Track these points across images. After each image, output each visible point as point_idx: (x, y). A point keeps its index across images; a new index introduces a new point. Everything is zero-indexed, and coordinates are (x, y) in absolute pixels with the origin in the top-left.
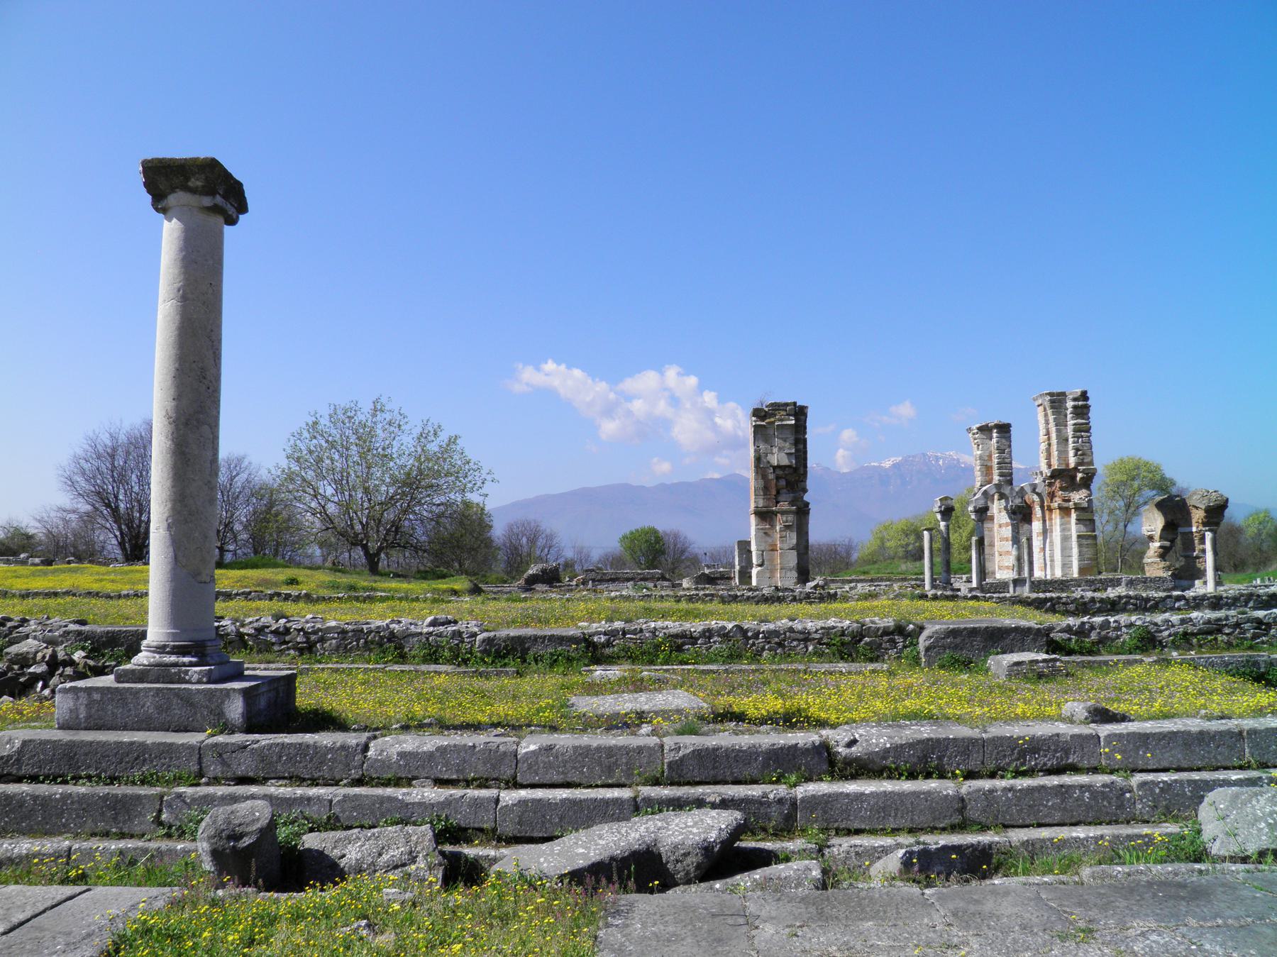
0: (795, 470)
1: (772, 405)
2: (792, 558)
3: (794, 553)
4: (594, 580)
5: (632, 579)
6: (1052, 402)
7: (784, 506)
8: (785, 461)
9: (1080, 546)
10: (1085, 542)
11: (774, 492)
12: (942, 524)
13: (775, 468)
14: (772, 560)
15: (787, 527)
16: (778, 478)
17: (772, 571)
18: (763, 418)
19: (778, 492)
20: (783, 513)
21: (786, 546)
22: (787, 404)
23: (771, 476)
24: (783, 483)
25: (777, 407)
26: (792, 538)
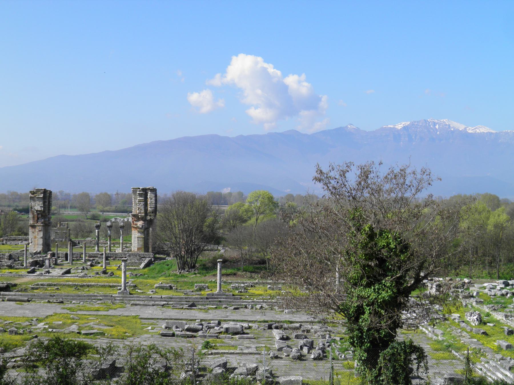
0: (44, 211)
1: (37, 190)
2: (41, 241)
3: (42, 239)
4: (6, 240)
5: (21, 240)
6: (133, 191)
7: (39, 224)
8: (39, 209)
9: (138, 240)
10: (140, 239)
11: (36, 219)
12: (97, 230)
13: (37, 211)
14: (35, 241)
15: (40, 231)
16: (38, 214)
17: (35, 245)
18: (33, 194)
19: (38, 219)
20: (38, 226)
21: (39, 237)
22: (42, 190)
23: (35, 214)
24: (40, 216)
25: (38, 190)
26: (41, 234)
